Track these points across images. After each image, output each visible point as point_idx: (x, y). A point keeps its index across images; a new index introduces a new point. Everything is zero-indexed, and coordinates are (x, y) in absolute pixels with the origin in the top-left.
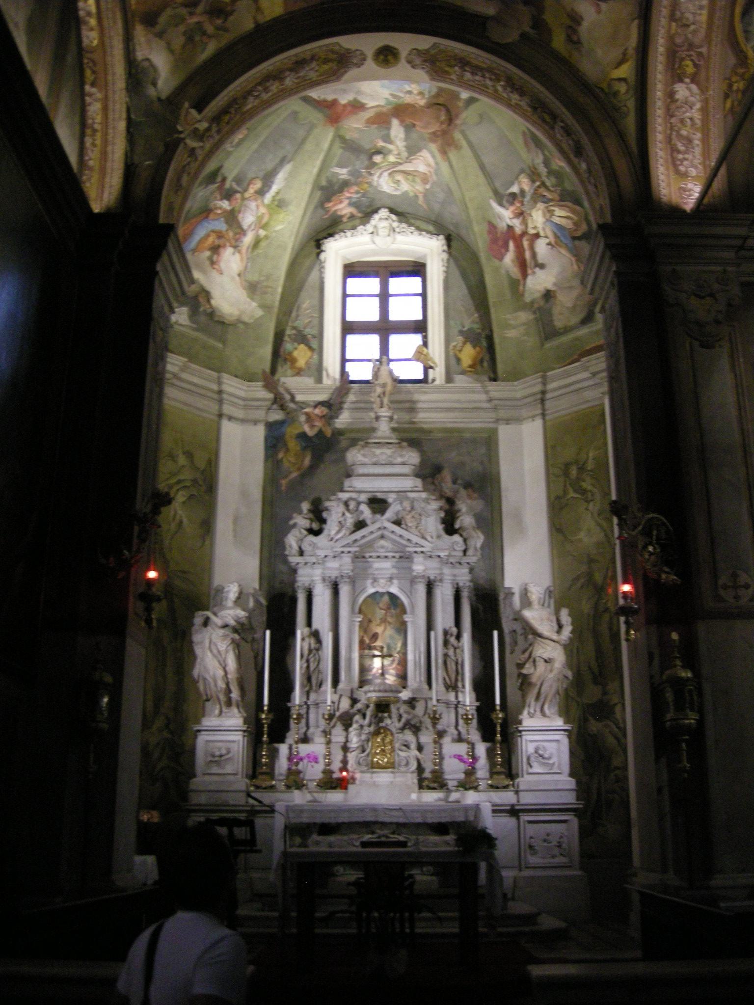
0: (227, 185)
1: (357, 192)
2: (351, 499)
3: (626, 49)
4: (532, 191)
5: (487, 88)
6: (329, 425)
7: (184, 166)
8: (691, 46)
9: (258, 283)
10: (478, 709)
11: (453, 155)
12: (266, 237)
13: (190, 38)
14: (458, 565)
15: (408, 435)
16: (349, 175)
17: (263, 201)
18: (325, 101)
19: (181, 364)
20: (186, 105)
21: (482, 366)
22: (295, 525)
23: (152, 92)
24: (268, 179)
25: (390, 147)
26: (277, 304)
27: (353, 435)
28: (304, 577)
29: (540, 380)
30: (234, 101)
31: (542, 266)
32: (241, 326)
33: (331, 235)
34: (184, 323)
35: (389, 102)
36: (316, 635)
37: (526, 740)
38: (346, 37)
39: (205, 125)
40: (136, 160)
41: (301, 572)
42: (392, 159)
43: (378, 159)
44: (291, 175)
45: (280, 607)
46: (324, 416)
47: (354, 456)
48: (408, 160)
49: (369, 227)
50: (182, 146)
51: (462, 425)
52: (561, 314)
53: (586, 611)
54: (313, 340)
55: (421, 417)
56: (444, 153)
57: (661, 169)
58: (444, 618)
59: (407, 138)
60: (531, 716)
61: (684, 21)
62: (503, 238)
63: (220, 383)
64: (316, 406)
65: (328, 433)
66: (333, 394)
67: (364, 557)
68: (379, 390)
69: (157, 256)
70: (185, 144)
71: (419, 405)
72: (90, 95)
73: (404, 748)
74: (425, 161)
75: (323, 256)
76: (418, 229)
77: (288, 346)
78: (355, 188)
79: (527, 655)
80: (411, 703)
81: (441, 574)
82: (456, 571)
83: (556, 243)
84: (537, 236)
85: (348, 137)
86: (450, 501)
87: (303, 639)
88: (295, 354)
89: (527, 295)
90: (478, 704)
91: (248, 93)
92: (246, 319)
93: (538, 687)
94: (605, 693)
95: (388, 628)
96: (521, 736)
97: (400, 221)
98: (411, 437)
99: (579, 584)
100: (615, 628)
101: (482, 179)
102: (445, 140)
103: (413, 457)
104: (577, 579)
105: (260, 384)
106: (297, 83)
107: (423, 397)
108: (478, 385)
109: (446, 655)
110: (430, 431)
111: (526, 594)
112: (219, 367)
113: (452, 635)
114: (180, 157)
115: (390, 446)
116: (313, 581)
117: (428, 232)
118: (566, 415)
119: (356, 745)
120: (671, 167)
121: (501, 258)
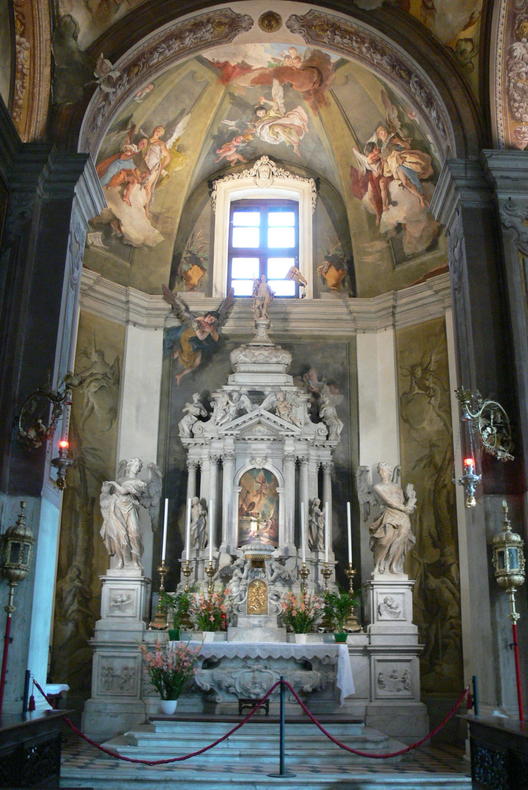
1: (243, 142)
2: (233, 391)
3: (473, 13)
4: (388, 141)
5: (353, 49)
6: (217, 331)
7: (100, 109)
9: (160, 214)
10: (337, 567)
11: (322, 111)
14: (322, 448)
15: (282, 341)
17: (166, 146)
18: (218, 63)
19: (95, 278)
20: (102, 55)
21: (344, 286)
22: (187, 412)
23: (72, 43)
24: (170, 128)
25: (271, 103)
26: (176, 231)
27: (236, 340)
28: (193, 456)
29: (392, 297)
30: (141, 56)
31: (395, 204)
33: (221, 177)
34: (98, 245)
35: (270, 65)
36: (204, 504)
37: (377, 593)
38: (237, 3)
39: (118, 74)
40: (59, 100)
41: (190, 451)
42: (272, 114)
43: (260, 113)
45: (175, 479)
46: (212, 324)
47: (237, 356)
48: (286, 115)
49: (253, 172)
50: (98, 90)
51: (327, 333)
52: (410, 243)
53: (427, 487)
54: (205, 263)
55: (293, 325)
56: (315, 108)
57: (500, 115)
58: (309, 491)
59: (285, 96)
60: (381, 572)
62: (361, 181)
63: (127, 295)
64: (206, 316)
65: (216, 338)
66: (220, 306)
67: (244, 439)
68: (258, 303)
69: (75, 181)
70: (101, 89)
71: (292, 316)
72: (20, 44)
73: (275, 597)
74: (300, 116)
75: (214, 194)
76: (292, 173)
77: (184, 266)
78: (242, 138)
79: (378, 522)
80: (281, 561)
81: (308, 454)
82: (320, 453)
83: (406, 184)
84: (391, 178)
85: (236, 95)
86: (316, 395)
87: (192, 507)
88: (190, 273)
89: (381, 227)
90: (336, 562)
92: (150, 244)
93: (387, 548)
94: (442, 555)
95: (263, 498)
96: (373, 589)
97: (278, 167)
98: (284, 342)
99: (422, 465)
100: (452, 502)
101: (347, 131)
102: (317, 98)
103: (286, 358)
104: (421, 460)
105: (161, 296)
106: (195, 44)
107: (295, 310)
108: (340, 301)
109: (310, 522)
110: (300, 338)
111: (379, 472)
112: (126, 281)
113: (315, 505)
114: (95, 100)
115: (267, 348)
116: (201, 459)
117: (300, 176)
118: (415, 325)
119: (235, 595)
120: (508, 115)
121: (361, 197)
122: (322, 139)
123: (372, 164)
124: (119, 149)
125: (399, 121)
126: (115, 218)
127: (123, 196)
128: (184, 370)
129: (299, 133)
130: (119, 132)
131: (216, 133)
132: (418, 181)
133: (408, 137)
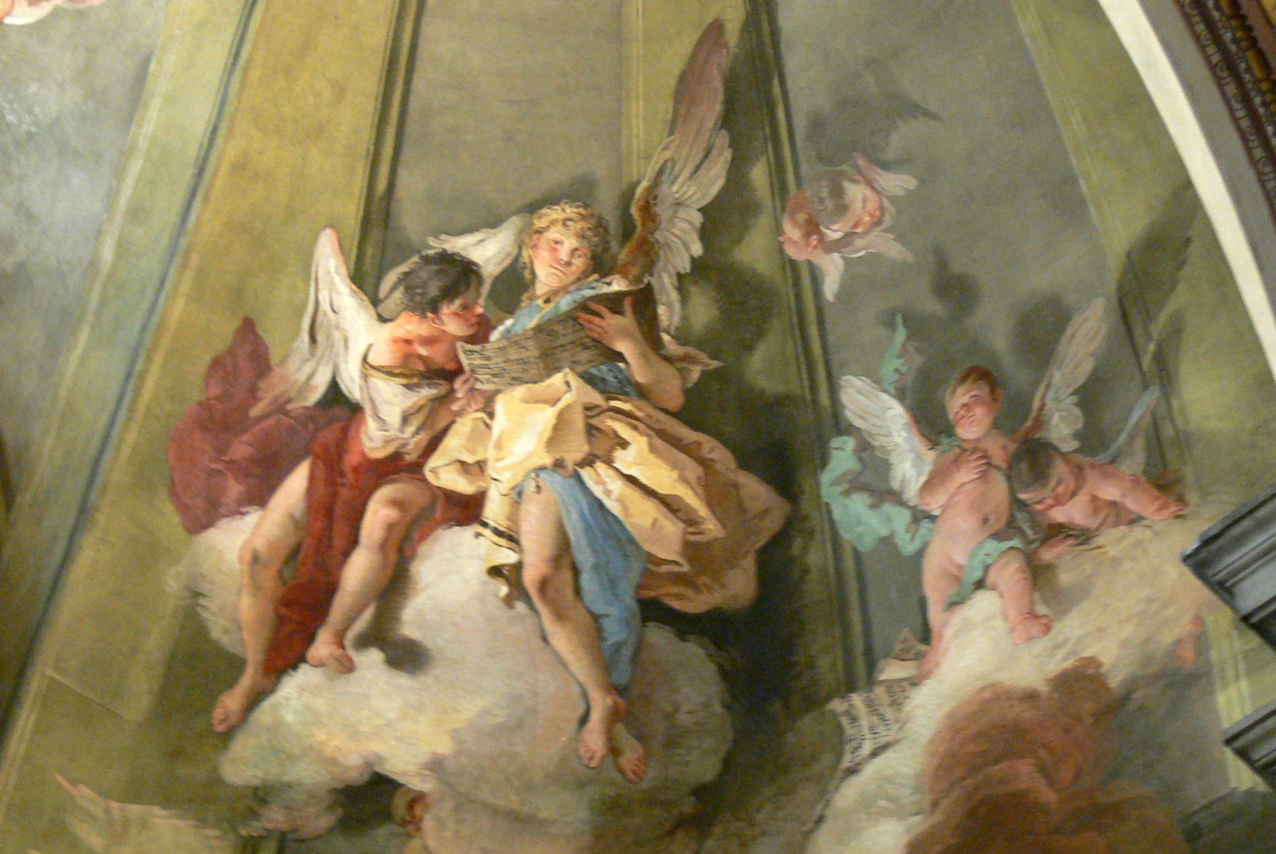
4: (565, 303)
31: (407, 657)
83: (543, 585)
84: (466, 510)
89: (243, 746)
101: (354, 118)
121: (202, 517)
122: (159, 85)
123: (389, 372)
125: (705, 234)
132: (629, 600)
133: (701, 344)
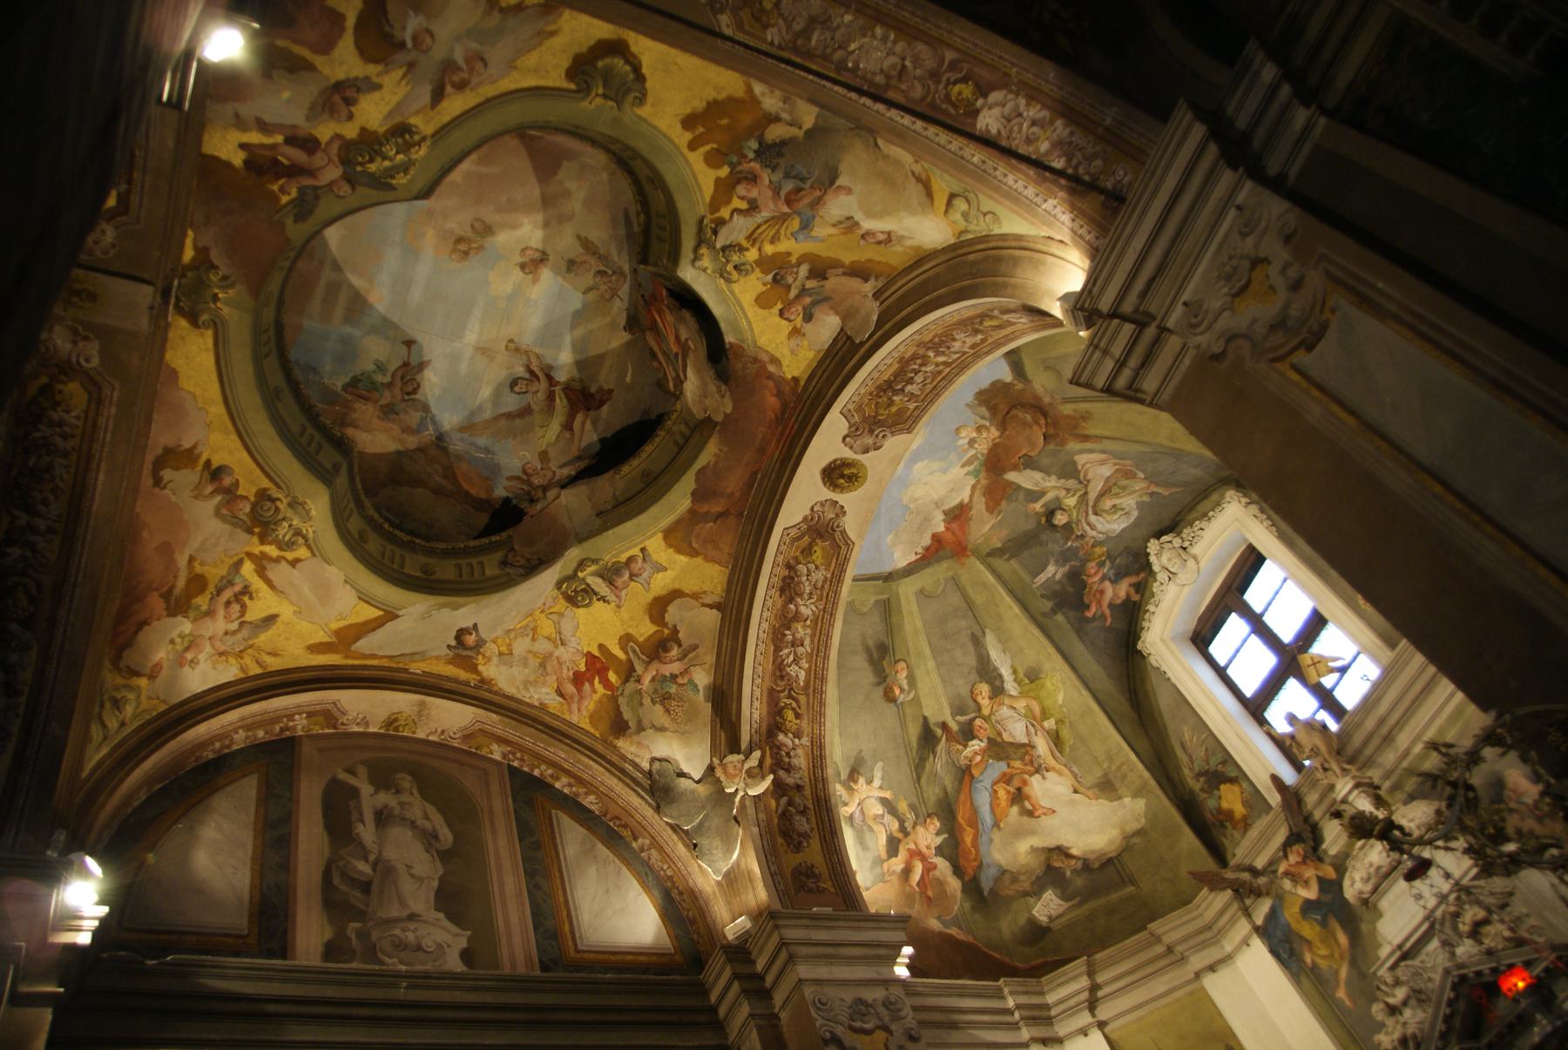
0: (954, 727)
1: (1101, 565)
8: (934, 75)
9: (1106, 775)
11: (1092, 429)
12: (1059, 722)
13: (664, 699)
16: (1063, 565)
18: (927, 549)
24: (987, 672)
26: (1146, 774)
32: (1136, 840)
35: (976, 473)
42: (1071, 502)
43: (1060, 519)
44: (1004, 641)
48: (1085, 483)
49: (1162, 577)
56: (1086, 438)
61: (894, 73)
64: (1286, 856)
76: (1204, 516)
85: (999, 545)
88: (1225, 805)
91: (780, 670)
92: (1135, 826)
105: (1205, 891)
124: (959, 768)
126: (1050, 850)
127: (1030, 814)
128: (1337, 972)
129: (1129, 475)
130: (934, 753)
131: (1049, 605)
